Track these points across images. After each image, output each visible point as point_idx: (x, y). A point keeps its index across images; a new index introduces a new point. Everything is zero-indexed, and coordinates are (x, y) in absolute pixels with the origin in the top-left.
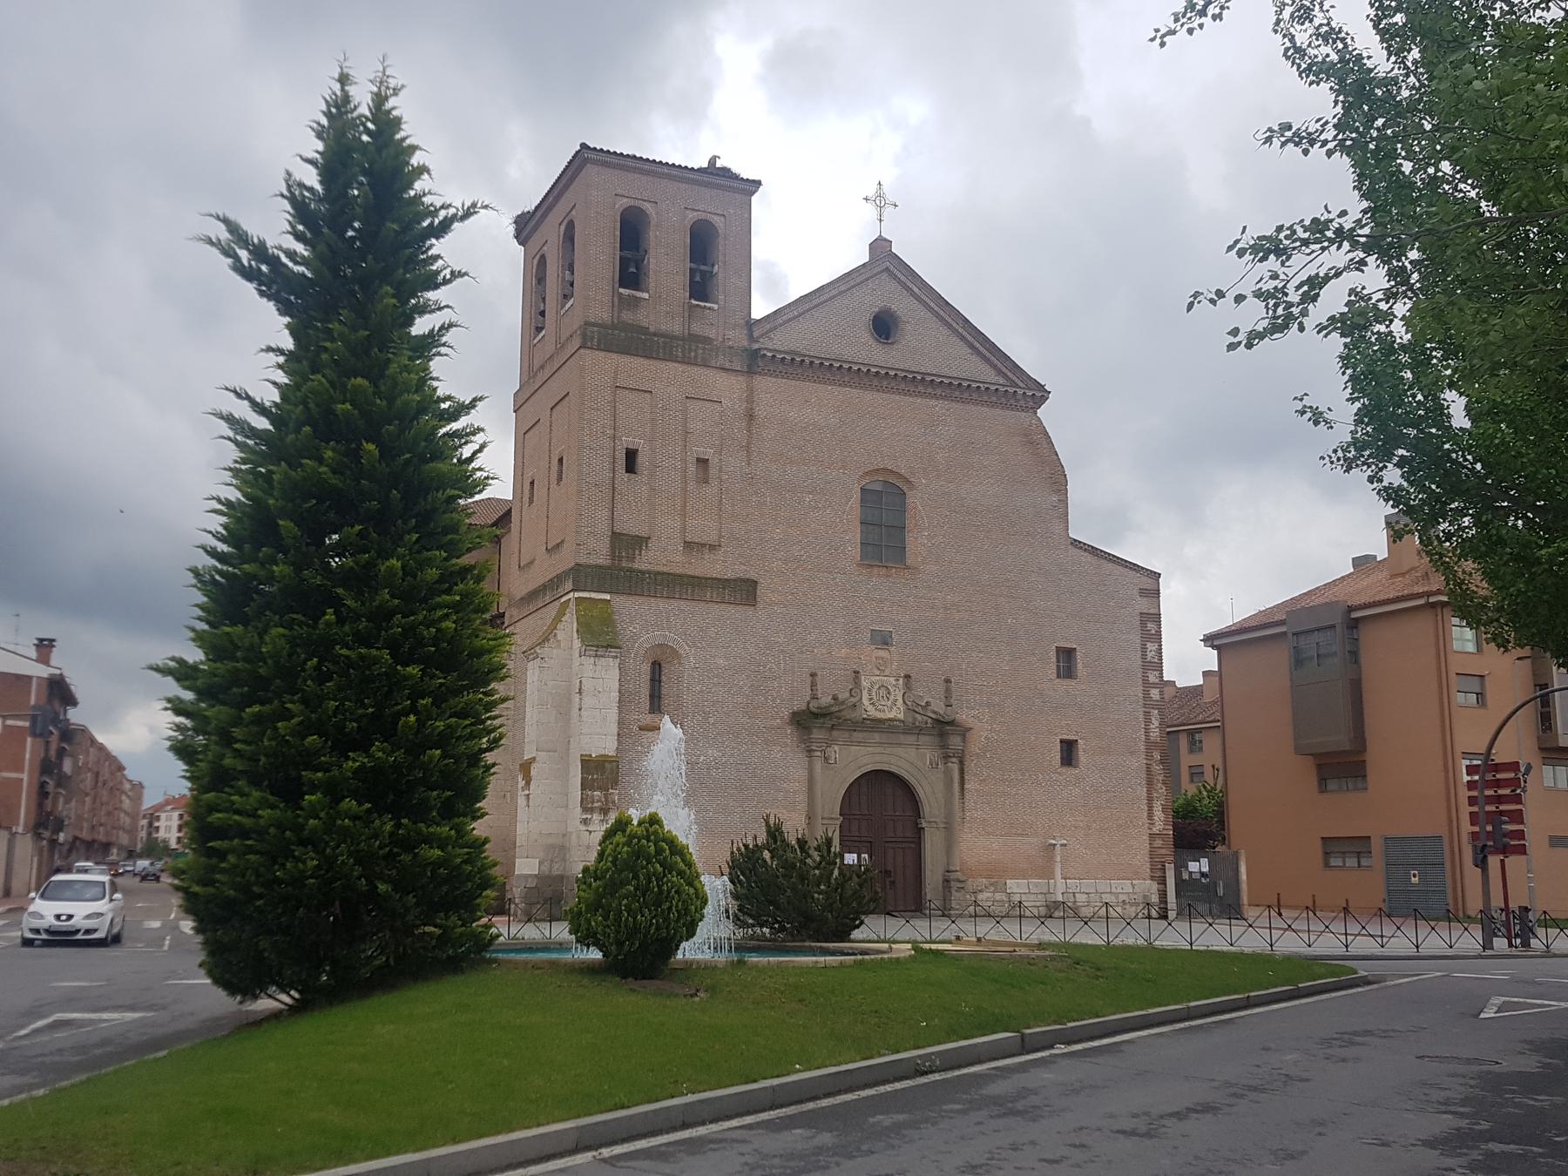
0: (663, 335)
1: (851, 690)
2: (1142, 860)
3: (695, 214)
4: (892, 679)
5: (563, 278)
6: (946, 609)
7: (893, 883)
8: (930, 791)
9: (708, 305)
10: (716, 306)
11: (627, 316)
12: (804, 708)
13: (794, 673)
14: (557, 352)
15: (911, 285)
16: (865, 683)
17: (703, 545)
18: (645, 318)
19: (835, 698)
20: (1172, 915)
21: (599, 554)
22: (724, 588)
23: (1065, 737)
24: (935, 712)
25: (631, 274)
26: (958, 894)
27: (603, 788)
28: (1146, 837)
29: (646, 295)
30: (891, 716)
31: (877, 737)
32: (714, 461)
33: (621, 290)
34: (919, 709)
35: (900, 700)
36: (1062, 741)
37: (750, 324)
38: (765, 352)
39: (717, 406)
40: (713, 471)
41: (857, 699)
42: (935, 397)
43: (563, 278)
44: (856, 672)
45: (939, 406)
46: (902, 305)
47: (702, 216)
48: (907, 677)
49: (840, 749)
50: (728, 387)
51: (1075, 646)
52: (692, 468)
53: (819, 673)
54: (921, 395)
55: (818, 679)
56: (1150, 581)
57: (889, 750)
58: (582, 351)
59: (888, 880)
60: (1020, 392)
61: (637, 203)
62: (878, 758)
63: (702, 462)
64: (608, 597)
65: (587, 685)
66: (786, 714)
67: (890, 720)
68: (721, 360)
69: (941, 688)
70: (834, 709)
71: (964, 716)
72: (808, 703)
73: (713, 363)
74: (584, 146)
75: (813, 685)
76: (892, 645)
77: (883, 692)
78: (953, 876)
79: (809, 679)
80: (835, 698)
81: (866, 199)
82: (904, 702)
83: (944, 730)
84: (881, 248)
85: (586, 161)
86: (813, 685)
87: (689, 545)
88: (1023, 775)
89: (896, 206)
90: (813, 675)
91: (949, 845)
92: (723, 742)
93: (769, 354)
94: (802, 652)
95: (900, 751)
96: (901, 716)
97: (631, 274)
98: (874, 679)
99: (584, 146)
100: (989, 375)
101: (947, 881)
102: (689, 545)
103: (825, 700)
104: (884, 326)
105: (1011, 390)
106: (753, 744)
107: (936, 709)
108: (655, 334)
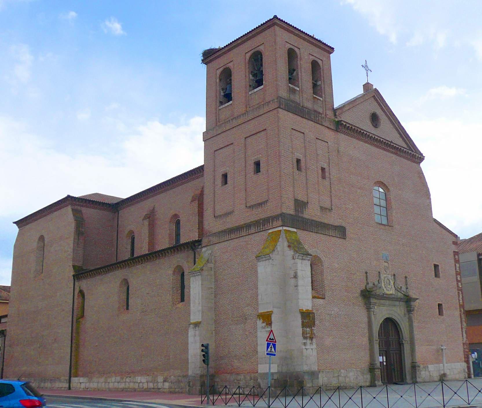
0: (307, 108)
2: (462, 355)
5: (249, 78)
8: (404, 326)
9: (319, 98)
10: (321, 99)
11: (292, 97)
12: (364, 289)
14: (246, 113)
15: (382, 104)
16: (382, 277)
17: (326, 209)
18: (297, 98)
19: (374, 284)
20: (473, 376)
21: (289, 209)
22: (335, 230)
25: (292, 78)
27: (310, 327)
28: (462, 344)
29: (298, 89)
31: (387, 302)
32: (327, 170)
33: (290, 85)
34: (399, 290)
37: (335, 111)
38: (343, 122)
39: (326, 144)
40: (327, 174)
42: (392, 153)
43: (249, 78)
46: (379, 112)
48: (394, 275)
50: (329, 135)
51: (438, 264)
52: (320, 171)
54: (388, 151)
56: (455, 238)
58: (279, 109)
63: (323, 169)
64: (295, 230)
65: (300, 274)
66: (359, 291)
67: (391, 294)
68: (327, 124)
69: (404, 280)
71: (413, 294)
72: (366, 286)
73: (324, 124)
74: (275, 17)
75: (367, 277)
80: (374, 284)
82: (394, 286)
83: (408, 300)
84: (367, 87)
85: (274, 24)
86: (367, 277)
87: (321, 208)
90: (366, 273)
91: (413, 351)
93: (345, 124)
95: (394, 308)
97: (292, 78)
99: (275, 17)
100: (405, 146)
102: (321, 208)
103: (371, 285)
104: (374, 119)
108: (305, 108)
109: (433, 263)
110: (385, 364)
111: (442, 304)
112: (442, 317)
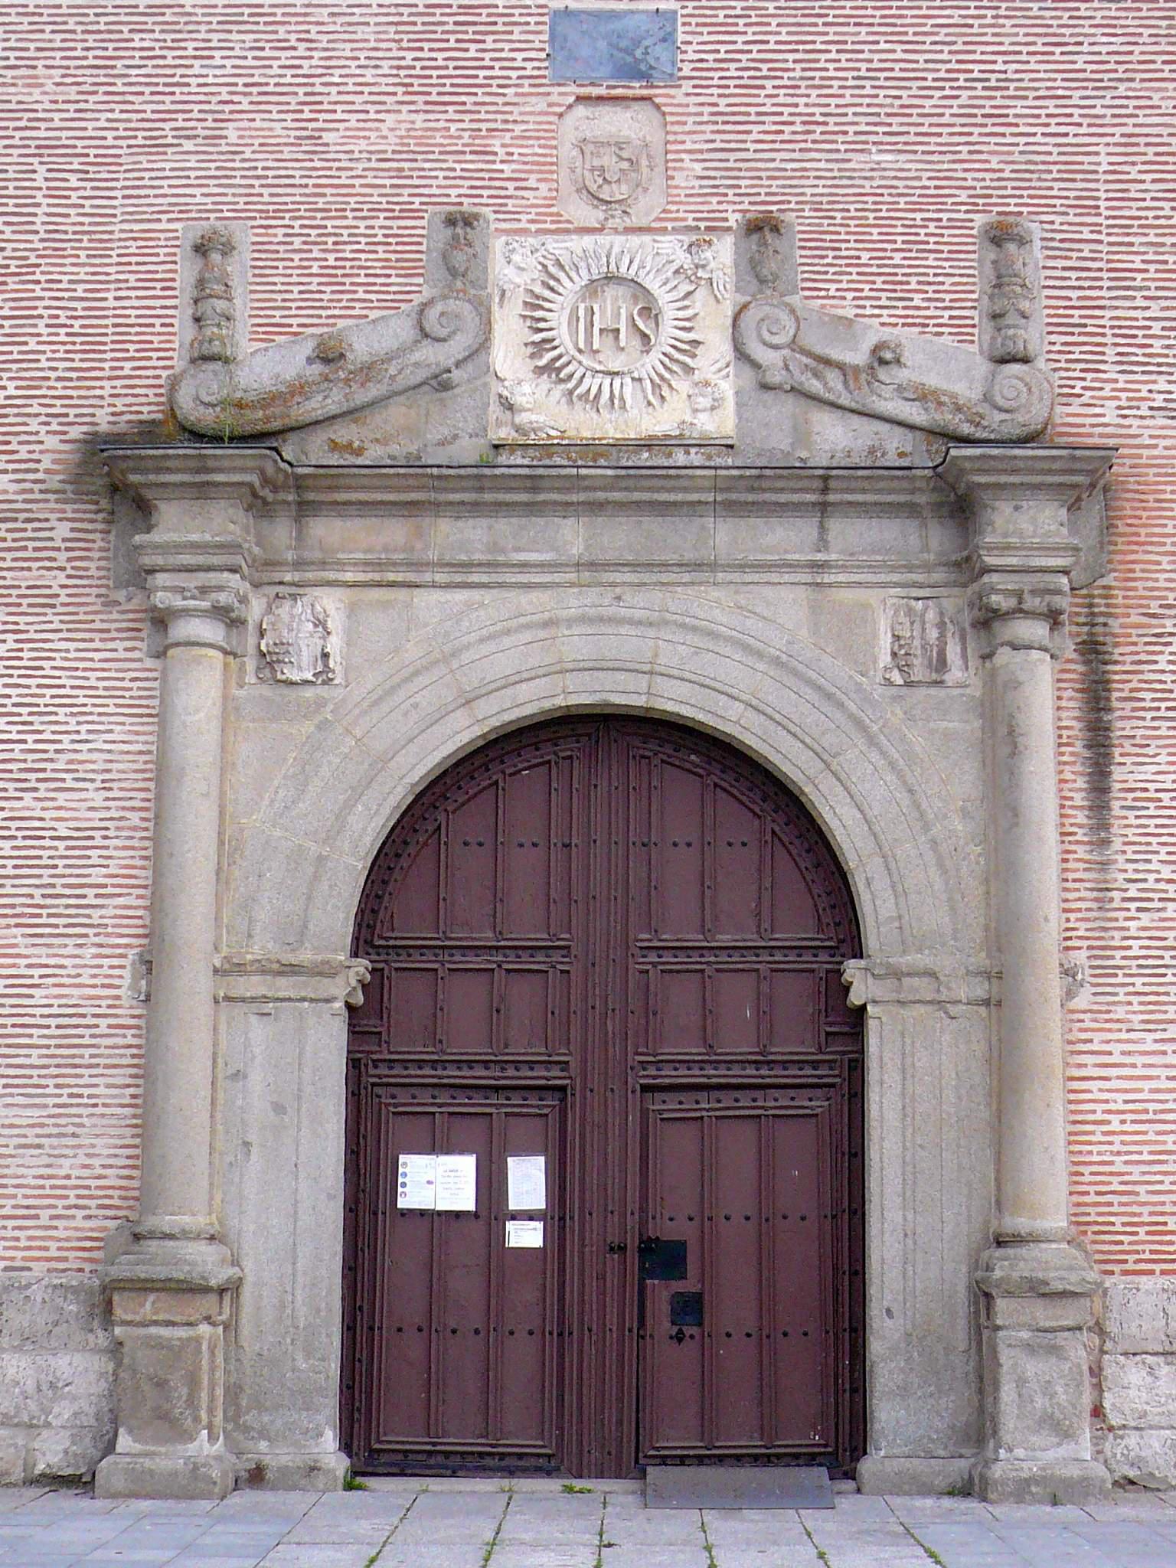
1: (424, 307)
4: (672, 247)
7: (689, 1308)
12: (148, 413)
13: (101, 246)
19: (329, 355)
24: (923, 396)
26: (1032, 1367)
30: (661, 422)
34: (833, 385)
35: (717, 348)
41: (457, 347)
44: (460, 221)
53: (245, 237)
55: (238, 268)
57: (639, 603)
59: (661, 1293)
62: (576, 646)
67: (648, 444)
70: (315, 406)
72: (174, 383)
76: (674, 80)
77: (614, 307)
78: (1006, 1267)
79: (185, 273)
80: (329, 355)
82: (741, 354)
94: (155, 146)
96: (721, 423)
98: (556, 246)
101: (983, 1297)
107: (933, 381)
110: (526, 1236)
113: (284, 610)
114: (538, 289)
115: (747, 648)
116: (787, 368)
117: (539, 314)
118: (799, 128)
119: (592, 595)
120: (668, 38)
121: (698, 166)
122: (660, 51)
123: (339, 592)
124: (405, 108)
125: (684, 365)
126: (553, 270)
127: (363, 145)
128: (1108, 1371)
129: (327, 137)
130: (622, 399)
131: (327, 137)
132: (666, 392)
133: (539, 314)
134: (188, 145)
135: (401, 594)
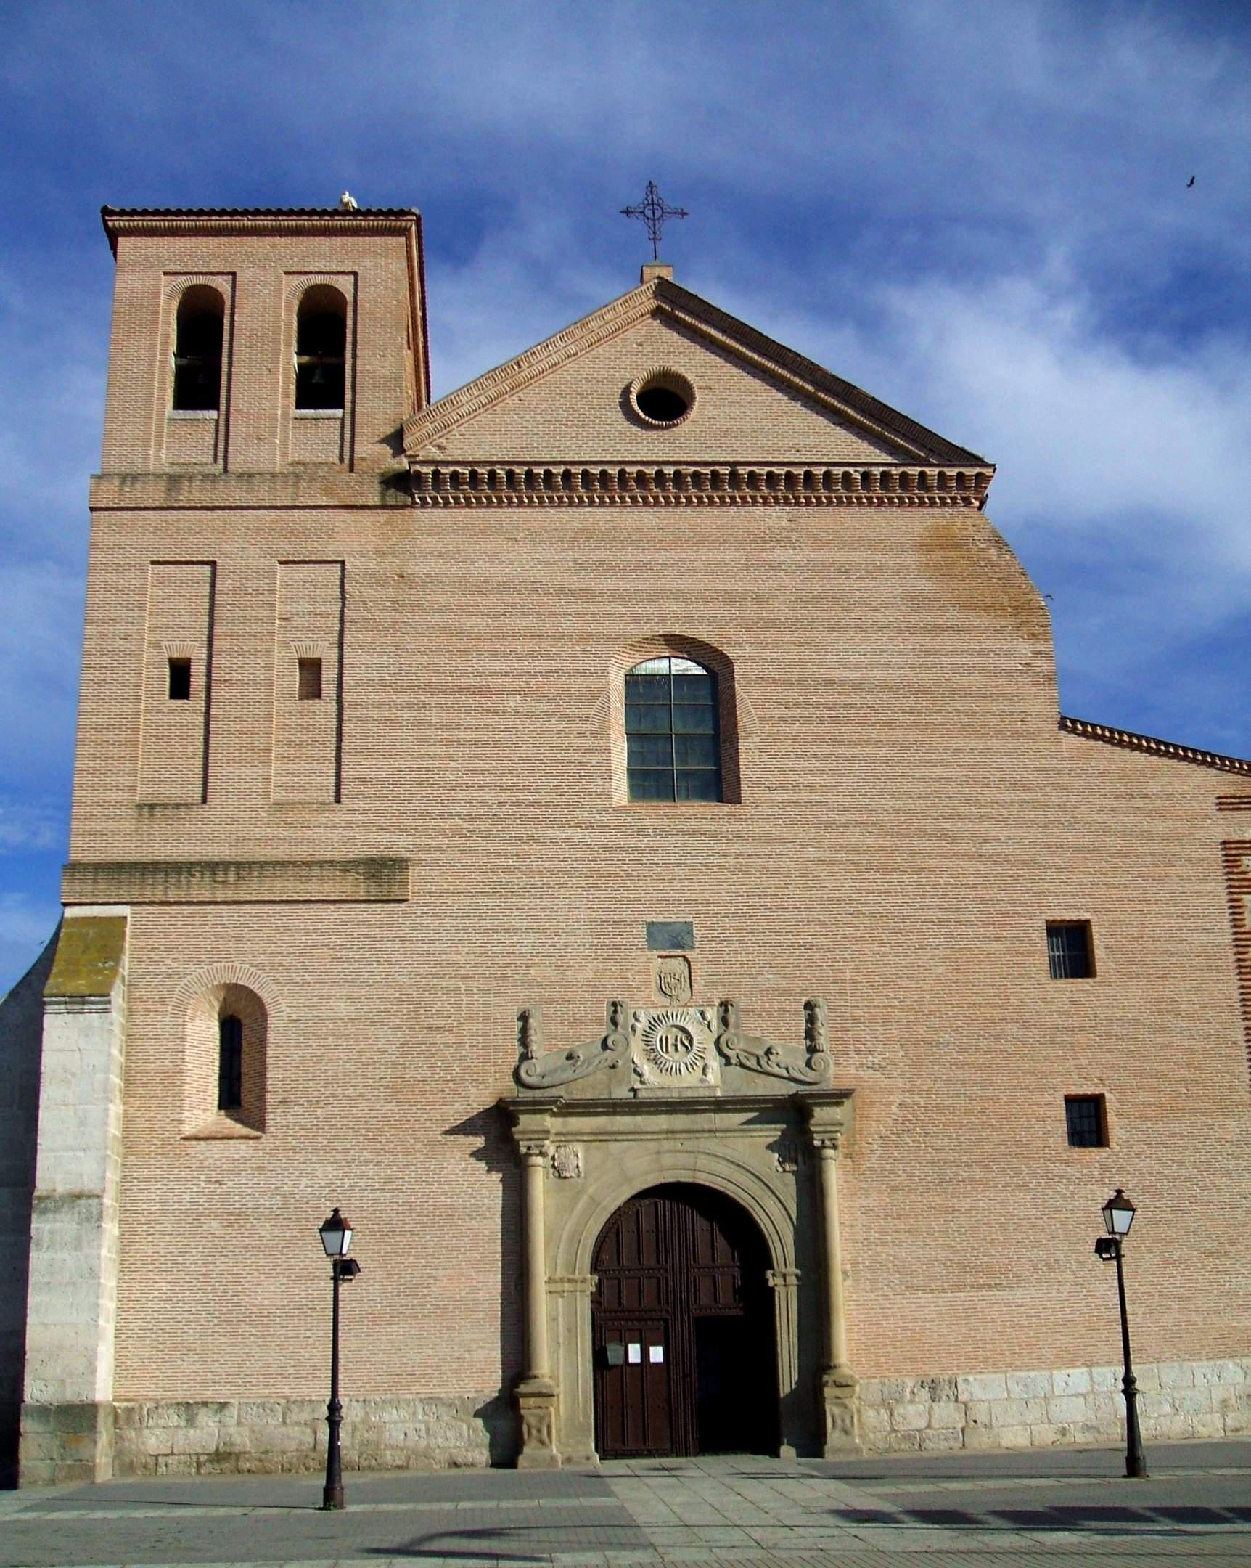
3: (304, 278)
6: (804, 871)
23: (1075, 1090)
36: (1069, 1100)
45: (774, 517)
47: (318, 279)
49: (587, 1151)
60: (932, 472)
61: (201, 280)
62: (668, 1160)
81: (627, 212)
88: (987, 1169)
89: (684, 214)
92: (346, 1152)
94: (505, 977)
105: (914, 471)
106: (407, 1151)
109: (1045, 917)
111: (1102, 1096)
112: (1094, 1154)
113: (562, 1150)
114: (648, 1030)
115: (728, 1160)
116: (738, 1057)
117: (649, 1039)
118: (738, 966)
119: (672, 1142)
120: (690, 933)
121: (702, 981)
122: (687, 937)
123: (581, 1144)
124: (595, 961)
125: (702, 1057)
126: (652, 1022)
127: (581, 976)
128: (863, 1411)
129: (567, 973)
130: (680, 1070)
131: (567, 973)
132: (695, 1067)
133: (649, 1039)
134: (517, 977)
135: (603, 1144)
